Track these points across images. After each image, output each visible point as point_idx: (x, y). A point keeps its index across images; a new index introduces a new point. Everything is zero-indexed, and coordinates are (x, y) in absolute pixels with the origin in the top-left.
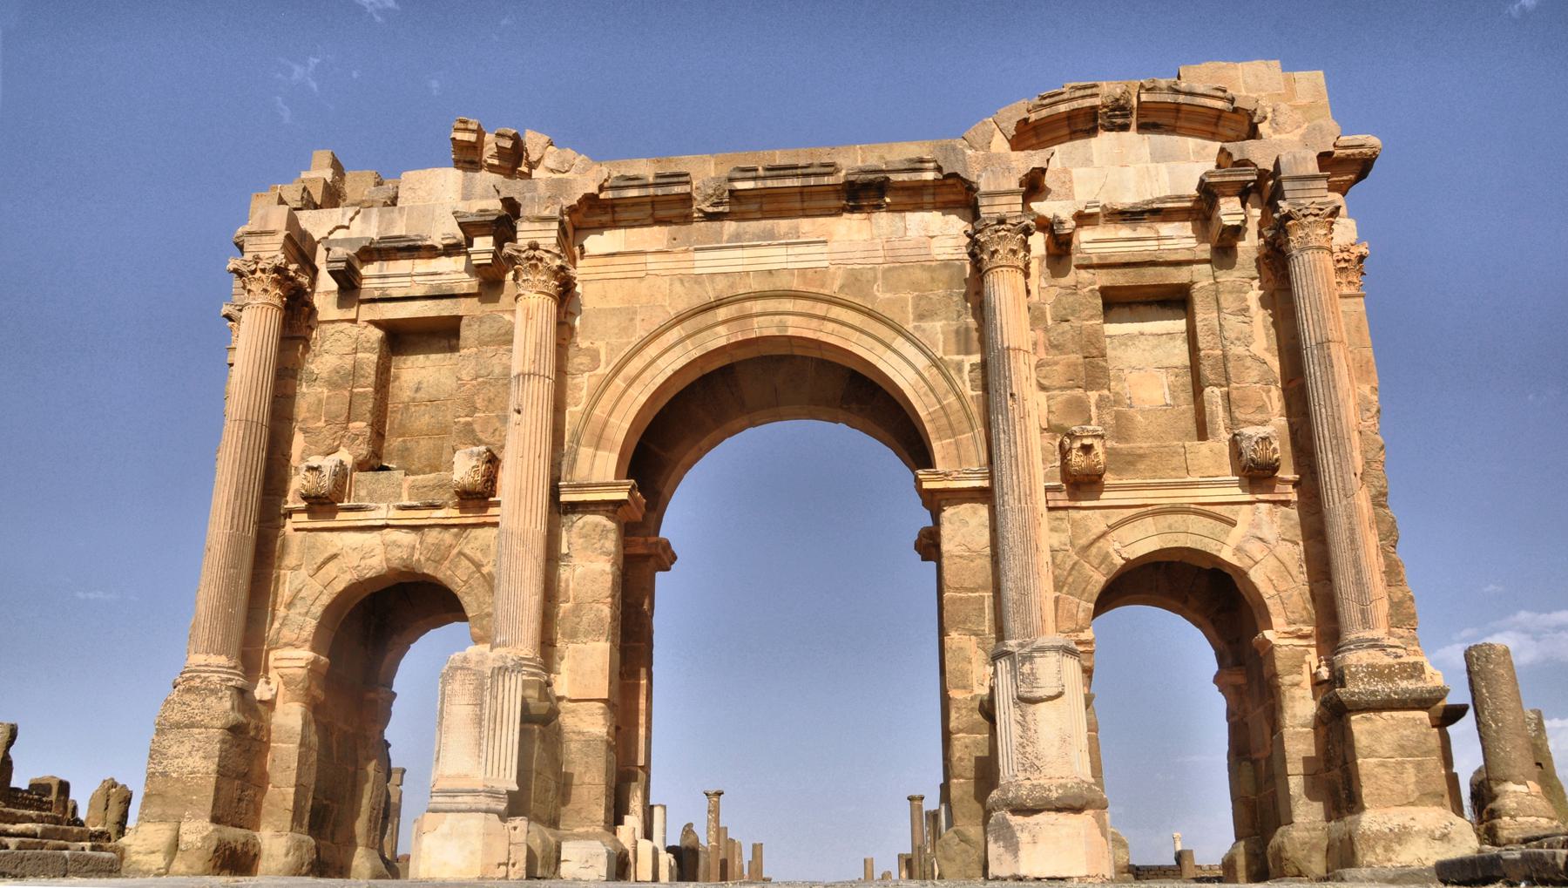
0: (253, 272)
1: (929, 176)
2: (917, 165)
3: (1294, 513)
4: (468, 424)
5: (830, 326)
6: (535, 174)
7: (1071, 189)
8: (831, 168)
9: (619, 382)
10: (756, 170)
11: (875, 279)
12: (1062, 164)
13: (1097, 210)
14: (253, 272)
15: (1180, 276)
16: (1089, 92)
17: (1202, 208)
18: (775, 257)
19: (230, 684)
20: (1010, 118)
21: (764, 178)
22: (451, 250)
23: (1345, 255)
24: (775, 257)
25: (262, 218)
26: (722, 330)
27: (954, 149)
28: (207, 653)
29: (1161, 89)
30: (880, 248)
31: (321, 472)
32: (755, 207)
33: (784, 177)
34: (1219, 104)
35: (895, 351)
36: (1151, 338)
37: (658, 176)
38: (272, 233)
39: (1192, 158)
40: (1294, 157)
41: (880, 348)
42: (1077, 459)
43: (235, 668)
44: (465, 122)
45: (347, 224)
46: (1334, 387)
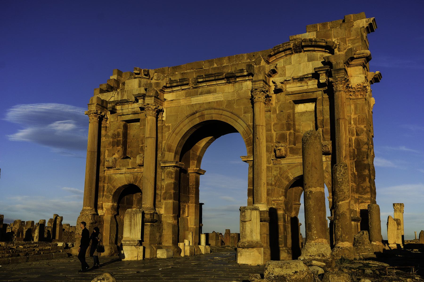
0: (90, 114)
1: (245, 73)
2: (242, 71)
4: (142, 146)
5: (223, 116)
7: (285, 72)
8: (222, 74)
9: (174, 135)
10: (203, 76)
11: (234, 103)
12: (283, 65)
13: (290, 79)
14: (90, 114)
15: (314, 96)
16: (288, 44)
18: (210, 98)
19: (91, 213)
20: (266, 55)
21: (205, 78)
23: (359, 86)
24: (210, 98)
25: (91, 100)
27: (251, 65)
28: (86, 207)
29: (307, 41)
30: (236, 94)
31: (109, 162)
32: (205, 85)
33: (210, 77)
35: (238, 123)
36: (309, 113)
37: (179, 80)
38: (93, 104)
39: (319, 59)
40: (337, 62)
41: (235, 122)
43: (92, 209)
44: (136, 68)
45: (114, 96)
46: (340, 132)
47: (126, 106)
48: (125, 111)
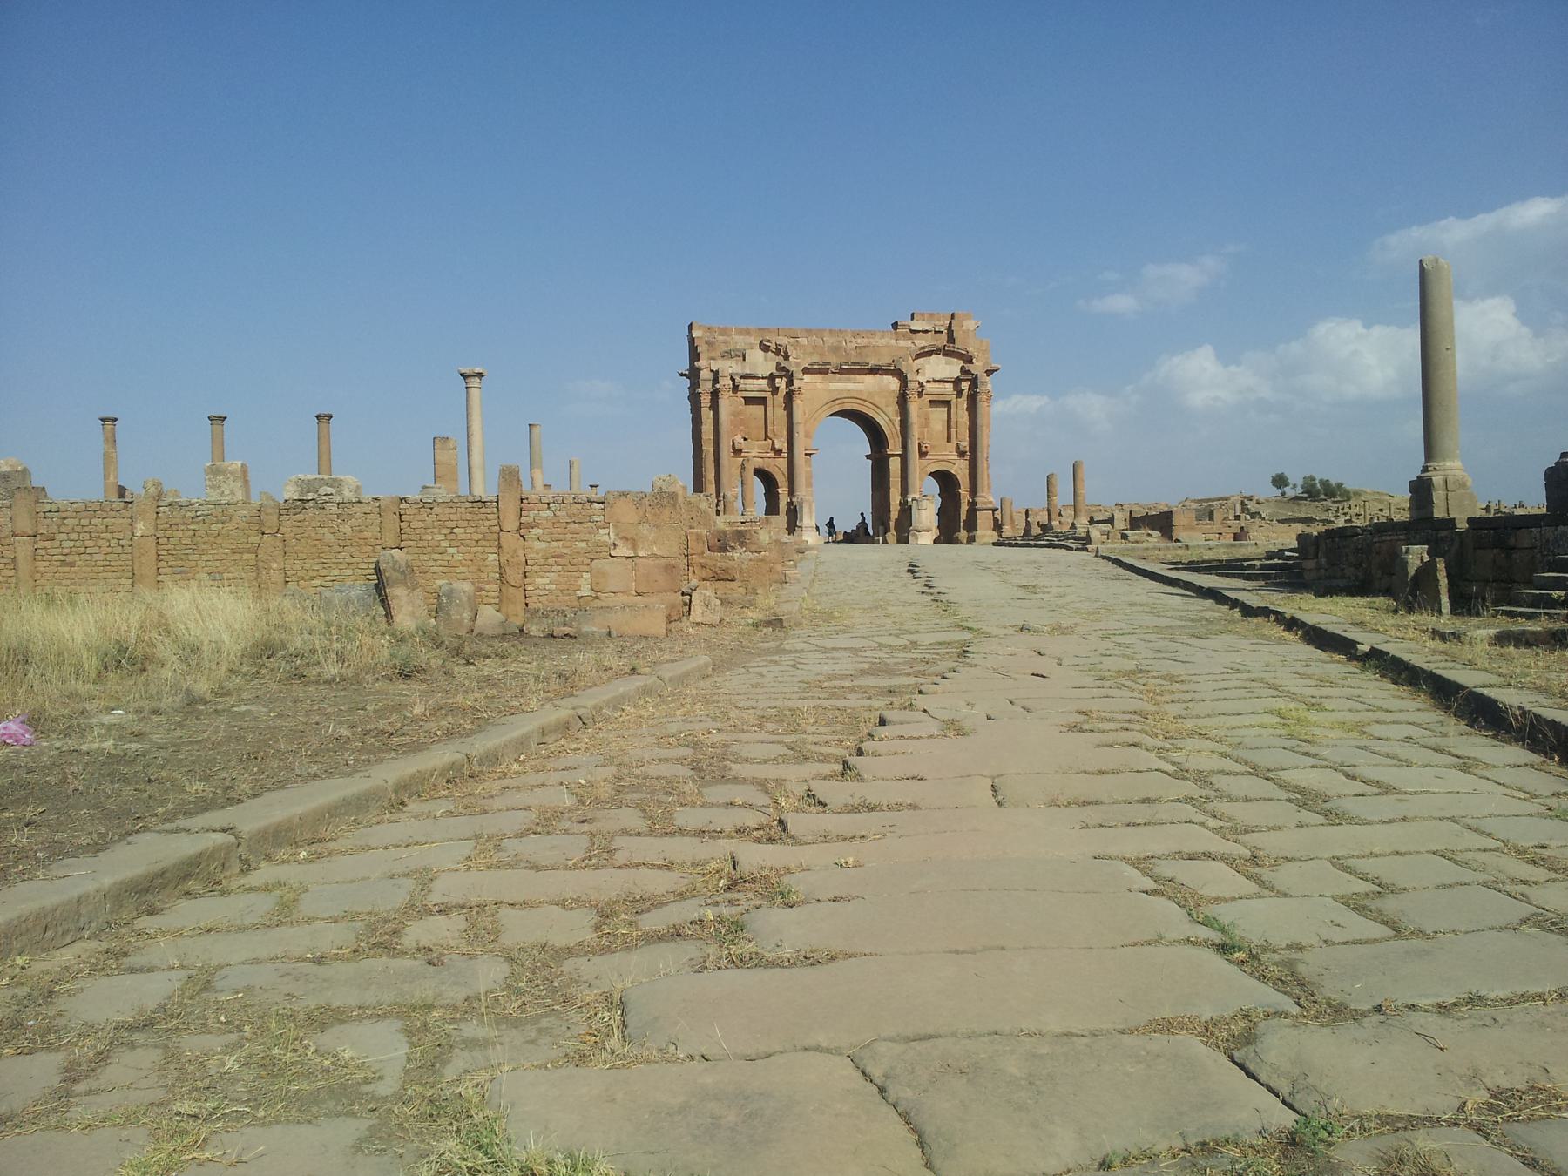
1: (892, 368)
2: (890, 365)
3: (967, 462)
6: (790, 358)
15: (948, 398)
17: (957, 382)
22: (763, 378)
26: (837, 406)
34: (964, 352)
42: (924, 449)
47: (750, 381)
48: (749, 387)
